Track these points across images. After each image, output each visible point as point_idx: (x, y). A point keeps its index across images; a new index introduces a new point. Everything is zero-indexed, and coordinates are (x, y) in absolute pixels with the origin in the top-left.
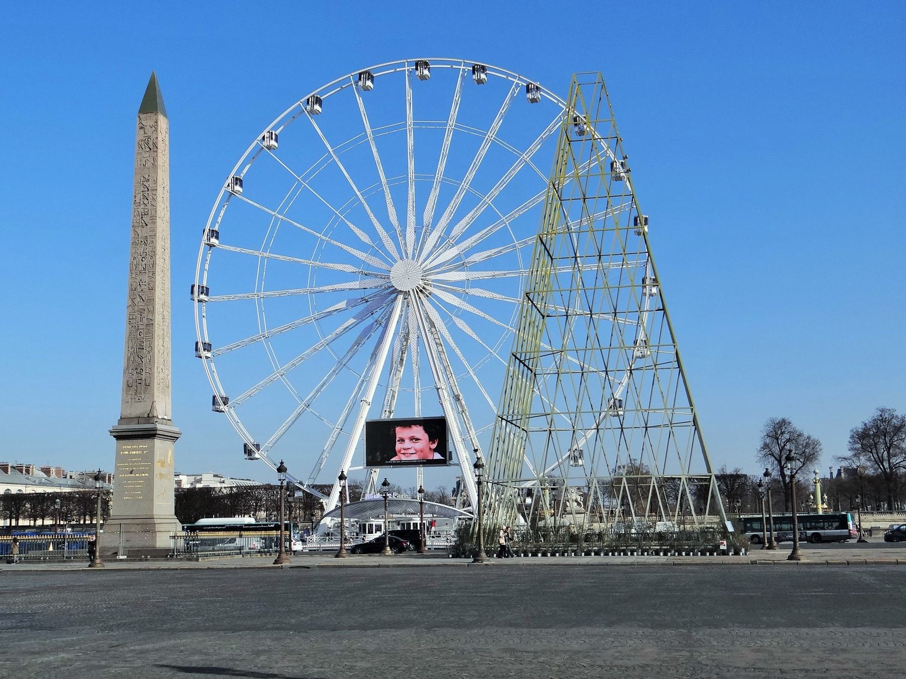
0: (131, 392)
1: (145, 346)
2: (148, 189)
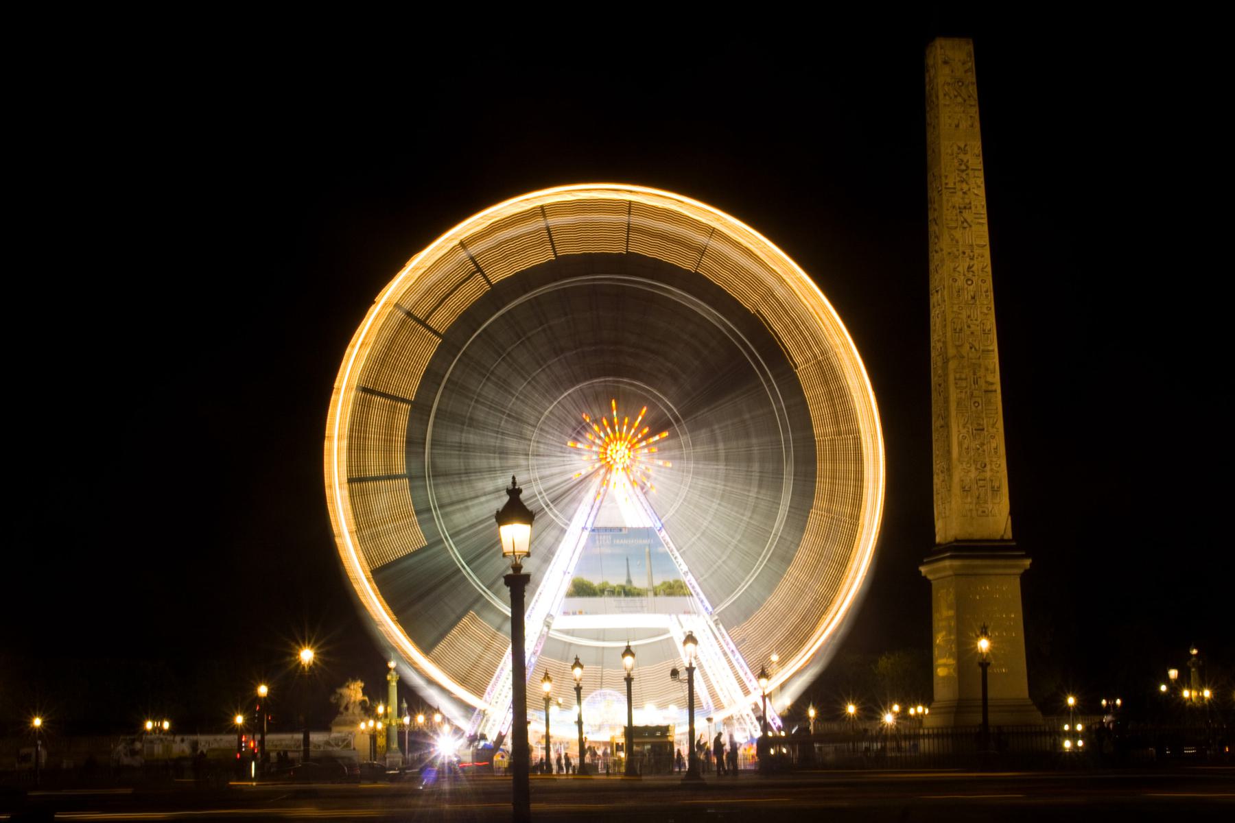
0: (969, 500)
1: (985, 426)
2: (967, 167)
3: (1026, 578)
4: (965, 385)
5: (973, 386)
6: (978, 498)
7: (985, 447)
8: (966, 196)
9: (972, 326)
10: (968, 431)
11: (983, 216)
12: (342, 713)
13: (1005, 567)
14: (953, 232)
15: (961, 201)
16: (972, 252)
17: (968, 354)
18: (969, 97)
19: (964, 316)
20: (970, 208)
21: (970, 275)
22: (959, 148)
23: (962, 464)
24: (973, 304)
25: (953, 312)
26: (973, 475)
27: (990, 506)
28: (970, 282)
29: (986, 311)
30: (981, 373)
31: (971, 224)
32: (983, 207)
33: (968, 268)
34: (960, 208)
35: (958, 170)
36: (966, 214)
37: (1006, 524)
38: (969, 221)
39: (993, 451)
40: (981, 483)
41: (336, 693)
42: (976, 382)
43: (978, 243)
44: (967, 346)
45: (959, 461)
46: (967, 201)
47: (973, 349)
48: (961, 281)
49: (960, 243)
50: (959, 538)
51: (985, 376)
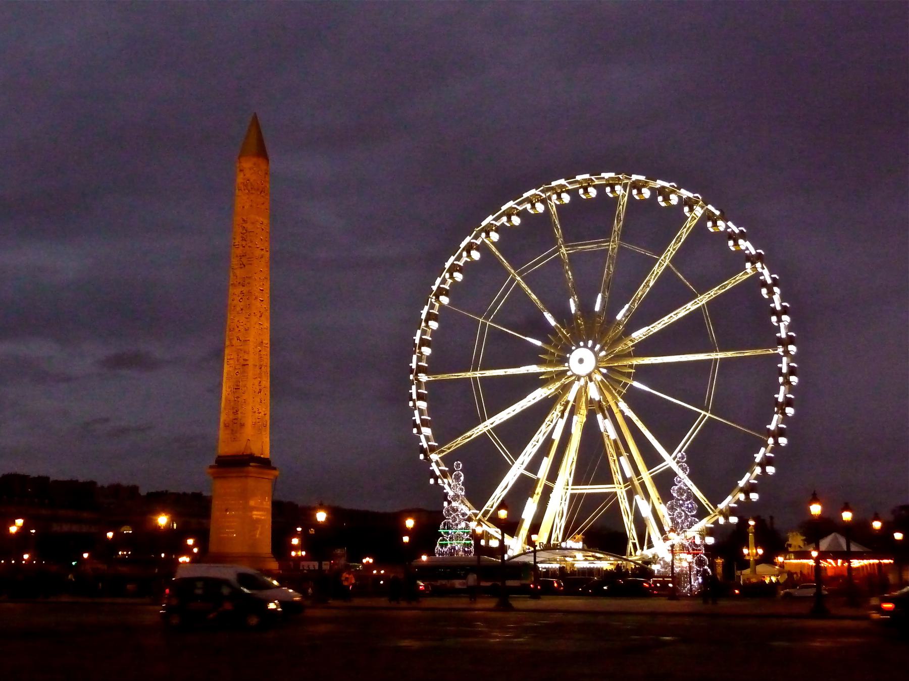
7: (239, 399)
9: (240, 327)
15: (241, 252)
18: (252, 188)
19: (236, 319)
22: (244, 220)
28: (241, 300)
30: (241, 355)
34: (240, 256)
35: (242, 233)
36: (244, 260)
38: (244, 263)
44: (236, 339)
46: (244, 251)
51: (243, 356)
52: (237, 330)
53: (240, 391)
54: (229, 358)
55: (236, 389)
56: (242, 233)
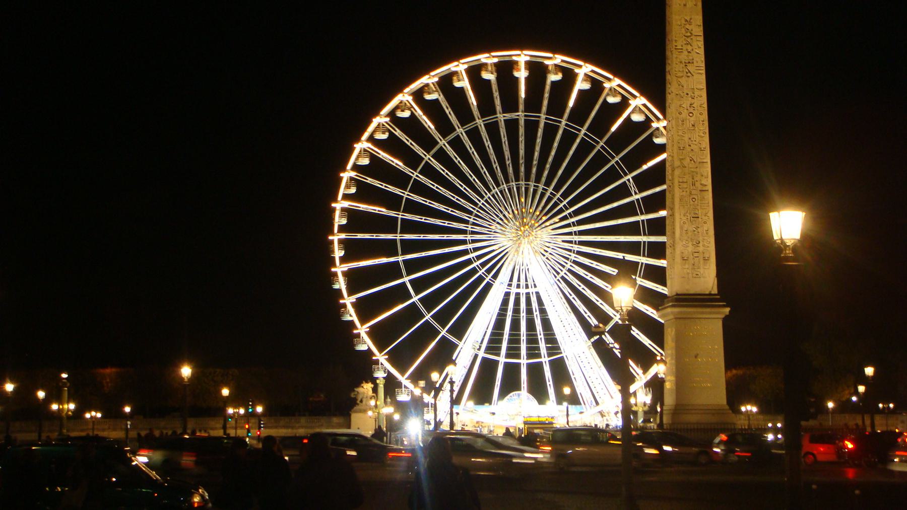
0: (687, 266)
1: (700, 214)
2: (691, 33)
3: (726, 321)
4: (686, 186)
5: (692, 187)
6: (694, 265)
8: (690, 54)
9: (692, 145)
10: (687, 219)
11: (702, 68)
12: (358, 404)
13: (710, 313)
14: (680, 80)
15: (686, 58)
16: (693, 93)
17: (689, 164)
20: (693, 63)
21: (691, 110)
22: (686, 21)
23: (682, 241)
24: (693, 130)
25: (678, 135)
26: (690, 248)
27: (702, 271)
28: (691, 115)
29: (703, 135)
31: (693, 74)
32: (702, 62)
33: (691, 105)
34: (685, 63)
35: (684, 36)
36: (690, 67)
37: (714, 282)
39: (705, 231)
40: (696, 255)
41: (354, 391)
42: (694, 184)
43: (698, 87)
44: (688, 159)
45: (680, 239)
46: (691, 58)
47: (692, 162)
48: (685, 114)
49: (685, 87)
50: (678, 293)
52: (688, 149)
53: (700, 219)
54: (681, 181)
55: (693, 217)
56: (684, 36)
